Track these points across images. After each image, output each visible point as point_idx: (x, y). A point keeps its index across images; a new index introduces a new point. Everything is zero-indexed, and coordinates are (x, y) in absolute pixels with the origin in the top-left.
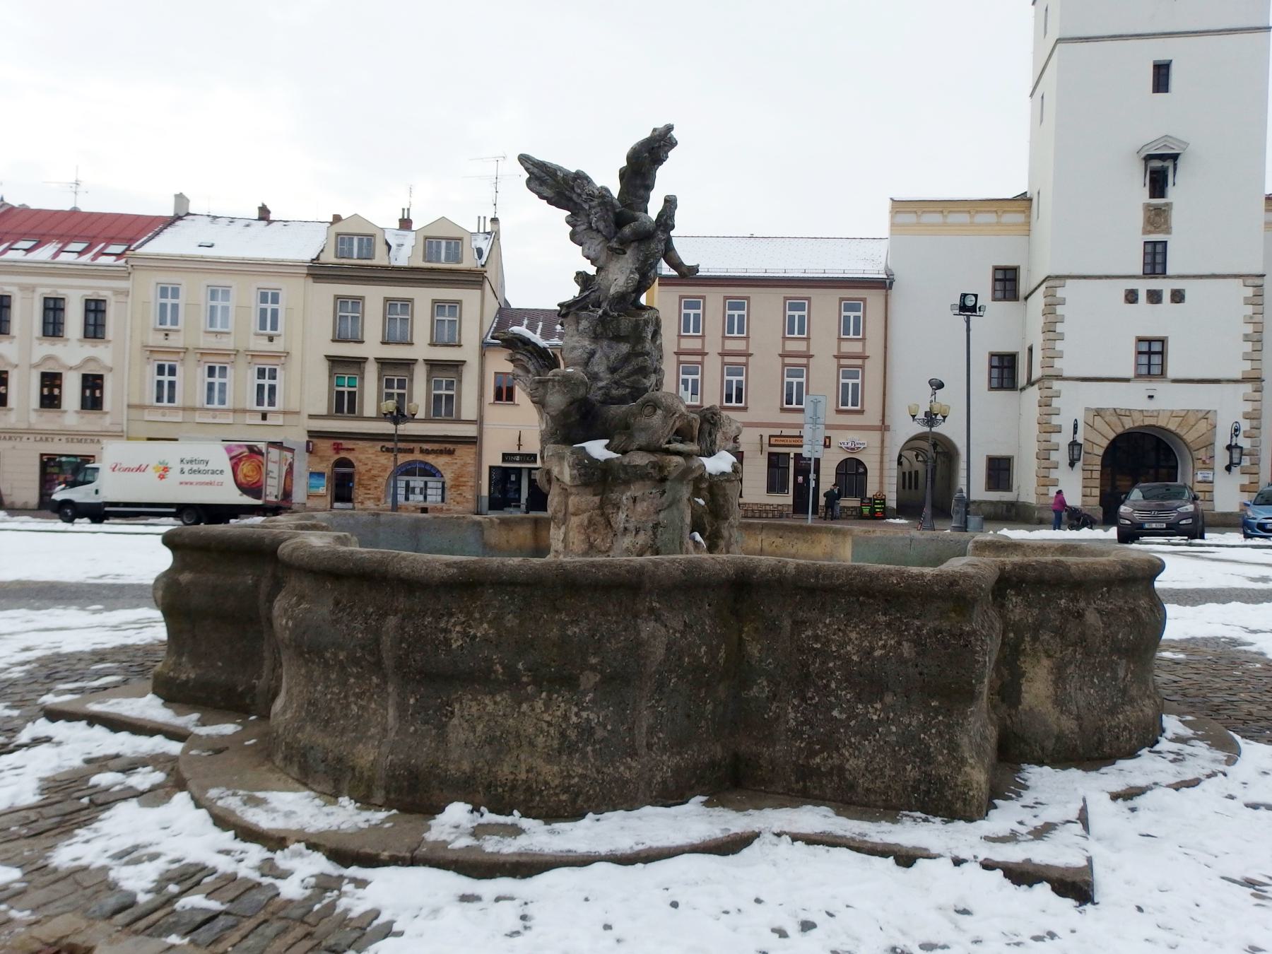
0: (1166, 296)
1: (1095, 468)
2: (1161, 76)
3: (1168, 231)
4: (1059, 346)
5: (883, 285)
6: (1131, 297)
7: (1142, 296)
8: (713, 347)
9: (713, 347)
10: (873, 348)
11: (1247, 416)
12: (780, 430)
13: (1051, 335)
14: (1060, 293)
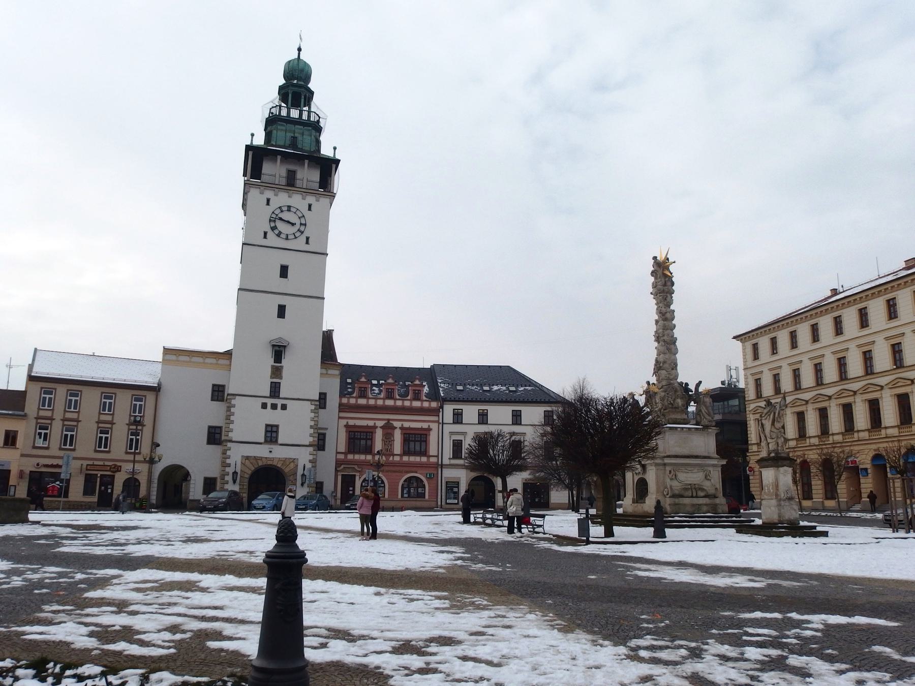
0: (279, 407)
1: (245, 484)
2: (282, 311)
3: (281, 378)
4: (231, 426)
5: (156, 390)
6: (264, 406)
7: (269, 406)
8: (58, 415)
9: (58, 415)
10: (148, 421)
11: (310, 461)
12: (92, 462)
13: (228, 421)
14: (233, 402)
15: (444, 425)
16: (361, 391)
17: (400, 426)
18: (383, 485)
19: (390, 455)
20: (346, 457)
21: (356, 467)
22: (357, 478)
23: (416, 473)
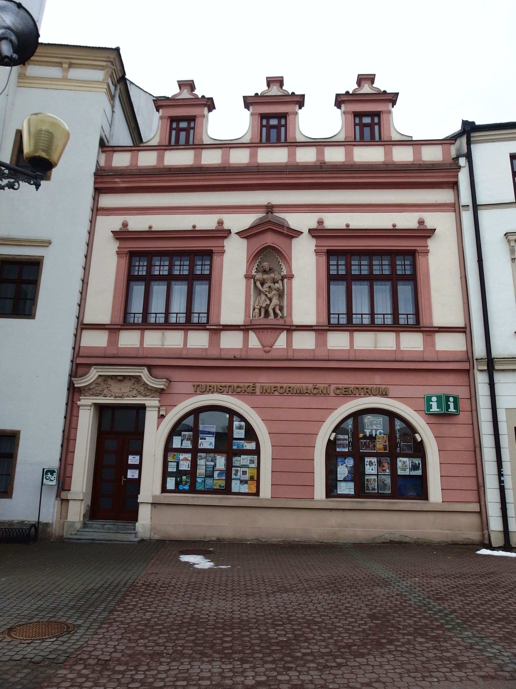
15: (483, 214)
16: (179, 130)
17: (314, 225)
18: (251, 446)
19: (278, 329)
20: (113, 341)
21: (144, 374)
22: (151, 417)
23: (385, 394)
